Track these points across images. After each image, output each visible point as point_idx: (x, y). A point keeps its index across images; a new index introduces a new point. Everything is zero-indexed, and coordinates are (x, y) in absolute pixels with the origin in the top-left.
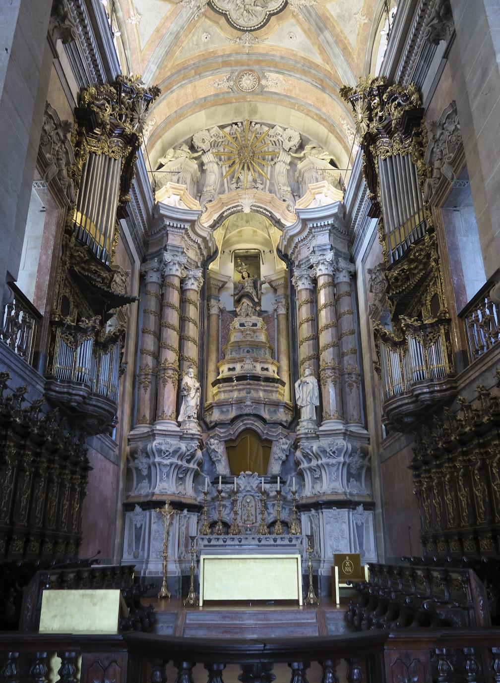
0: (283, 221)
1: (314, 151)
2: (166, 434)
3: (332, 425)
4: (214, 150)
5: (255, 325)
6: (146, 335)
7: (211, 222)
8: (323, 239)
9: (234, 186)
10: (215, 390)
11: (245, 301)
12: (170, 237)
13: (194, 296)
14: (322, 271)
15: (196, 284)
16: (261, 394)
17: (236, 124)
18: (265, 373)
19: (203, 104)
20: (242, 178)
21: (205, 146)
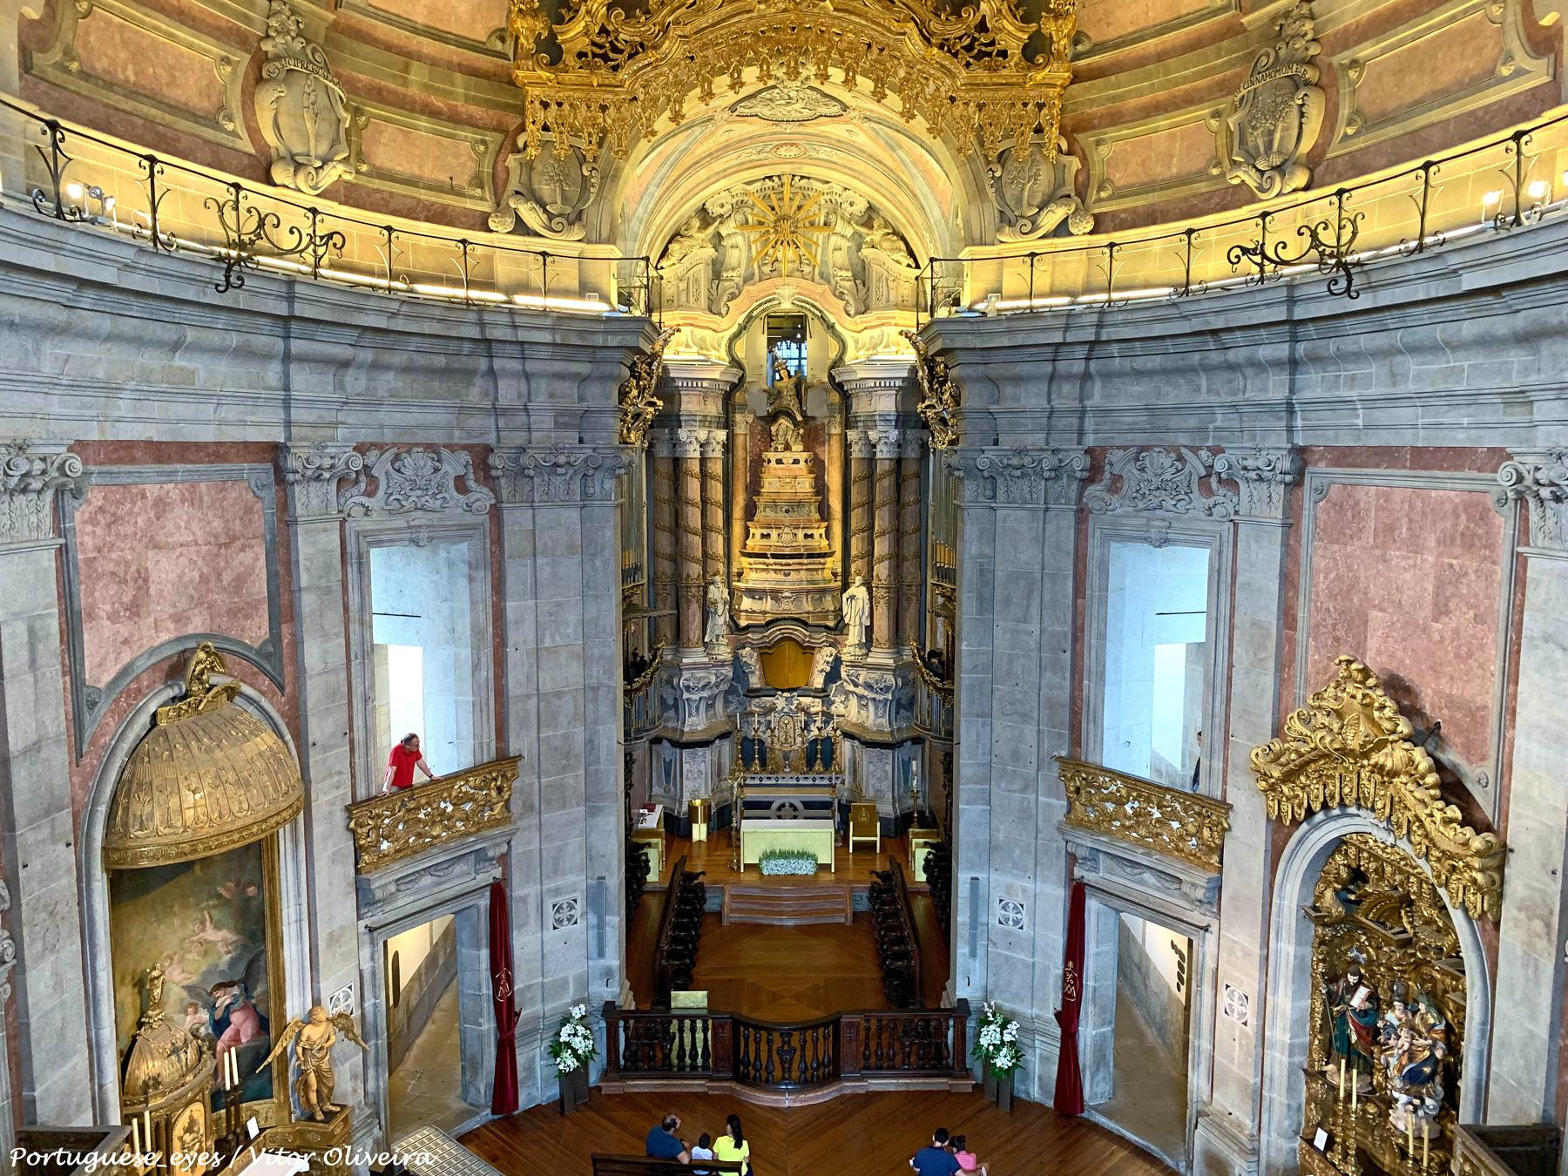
0: (838, 327)
1: (885, 245)
2: (695, 667)
3: (881, 656)
4: (740, 217)
5: (796, 462)
6: (660, 533)
7: (735, 329)
8: (886, 404)
9: (767, 269)
10: (745, 561)
11: (784, 422)
12: (684, 399)
13: (717, 468)
14: (883, 452)
15: (719, 447)
16: (803, 575)
17: (770, 178)
18: (809, 542)
19: (724, 173)
20: (780, 255)
21: (722, 211)
